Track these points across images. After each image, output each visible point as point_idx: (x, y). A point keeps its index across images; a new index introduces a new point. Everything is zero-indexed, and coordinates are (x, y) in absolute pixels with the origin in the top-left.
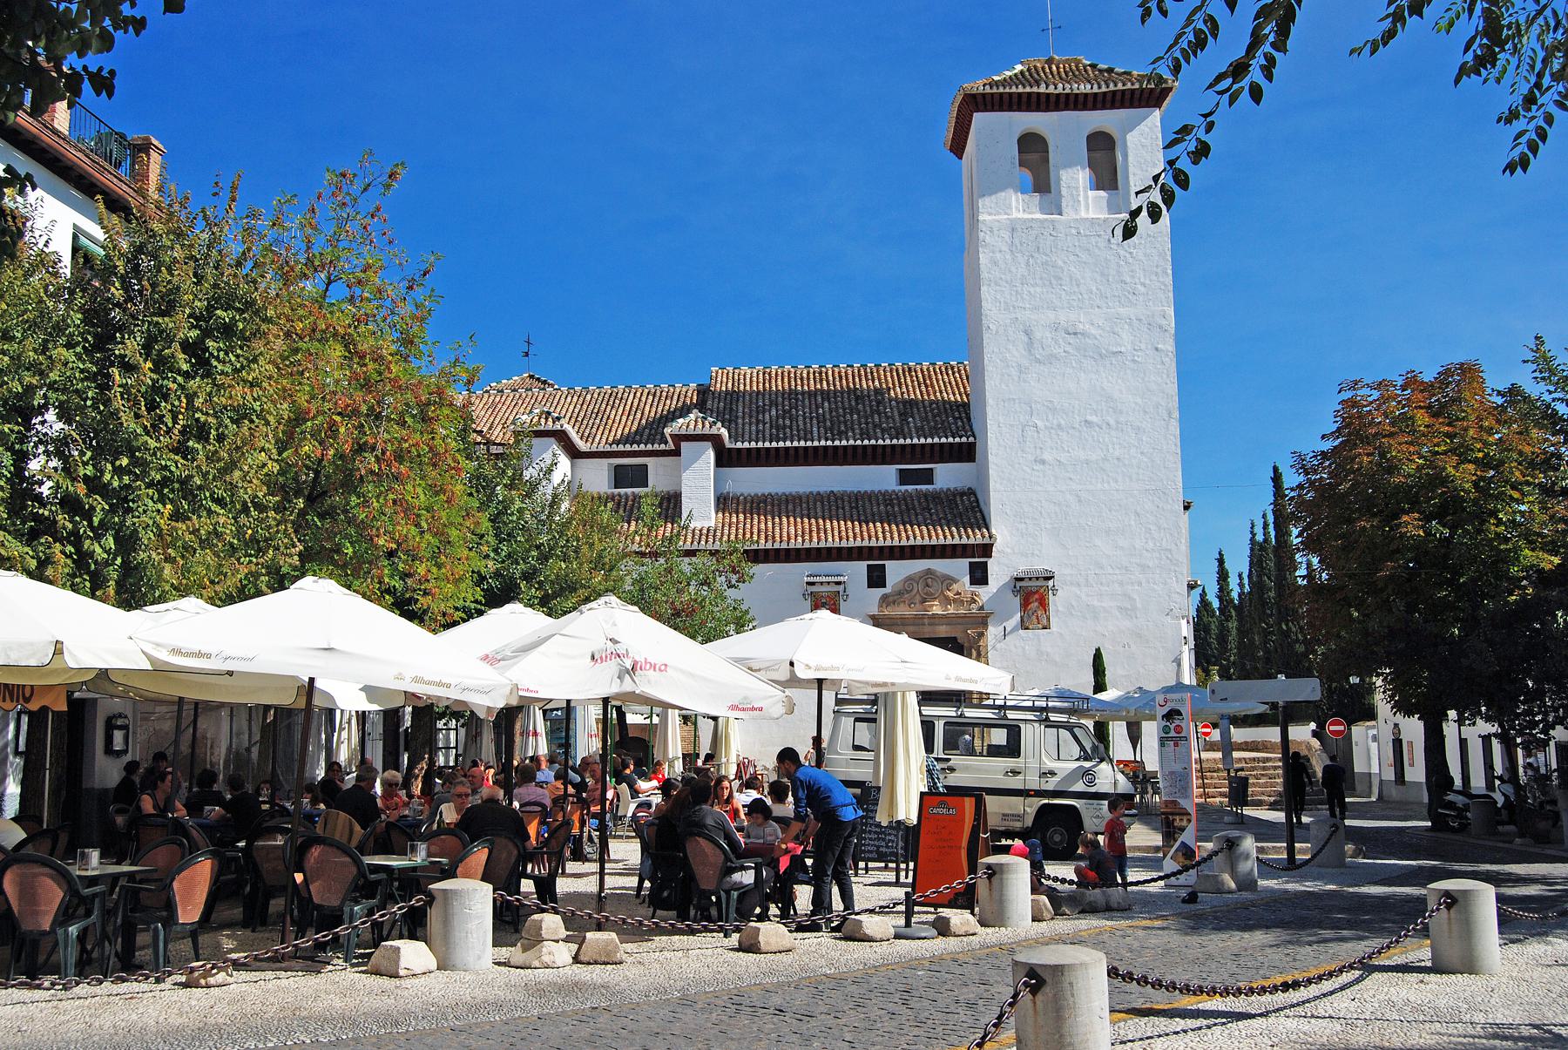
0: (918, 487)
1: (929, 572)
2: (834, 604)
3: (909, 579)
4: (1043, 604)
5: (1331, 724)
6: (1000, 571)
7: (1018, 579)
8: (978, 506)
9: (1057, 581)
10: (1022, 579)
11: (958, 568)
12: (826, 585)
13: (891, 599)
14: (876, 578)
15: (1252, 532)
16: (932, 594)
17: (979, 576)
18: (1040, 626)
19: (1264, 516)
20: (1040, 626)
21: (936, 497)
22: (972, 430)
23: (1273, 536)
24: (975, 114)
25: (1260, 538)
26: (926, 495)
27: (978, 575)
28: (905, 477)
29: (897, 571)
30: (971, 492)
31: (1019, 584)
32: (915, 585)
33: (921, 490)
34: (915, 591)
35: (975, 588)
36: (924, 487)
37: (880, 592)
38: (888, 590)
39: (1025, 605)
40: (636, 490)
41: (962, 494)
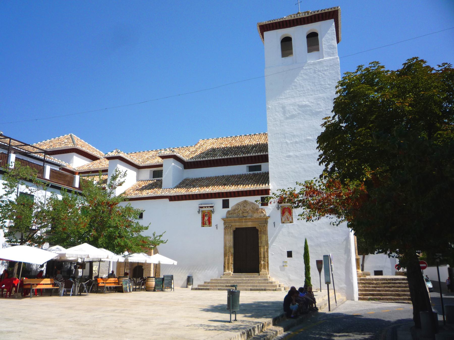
0: (254, 172)
1: (245, 202)
2: (210, 215)
3: (238, 205)
13: (231, 212)
14: (226, 205)
16: (246, 210)
18: (289, 222)
20: (289, 222)
28: (251, 169)
29: (233, 202)
32: (240, 207)
33: (255, 173)
35: (263, 207)
36: (256, 172)
37: (226, 210)
39: (283, 213)
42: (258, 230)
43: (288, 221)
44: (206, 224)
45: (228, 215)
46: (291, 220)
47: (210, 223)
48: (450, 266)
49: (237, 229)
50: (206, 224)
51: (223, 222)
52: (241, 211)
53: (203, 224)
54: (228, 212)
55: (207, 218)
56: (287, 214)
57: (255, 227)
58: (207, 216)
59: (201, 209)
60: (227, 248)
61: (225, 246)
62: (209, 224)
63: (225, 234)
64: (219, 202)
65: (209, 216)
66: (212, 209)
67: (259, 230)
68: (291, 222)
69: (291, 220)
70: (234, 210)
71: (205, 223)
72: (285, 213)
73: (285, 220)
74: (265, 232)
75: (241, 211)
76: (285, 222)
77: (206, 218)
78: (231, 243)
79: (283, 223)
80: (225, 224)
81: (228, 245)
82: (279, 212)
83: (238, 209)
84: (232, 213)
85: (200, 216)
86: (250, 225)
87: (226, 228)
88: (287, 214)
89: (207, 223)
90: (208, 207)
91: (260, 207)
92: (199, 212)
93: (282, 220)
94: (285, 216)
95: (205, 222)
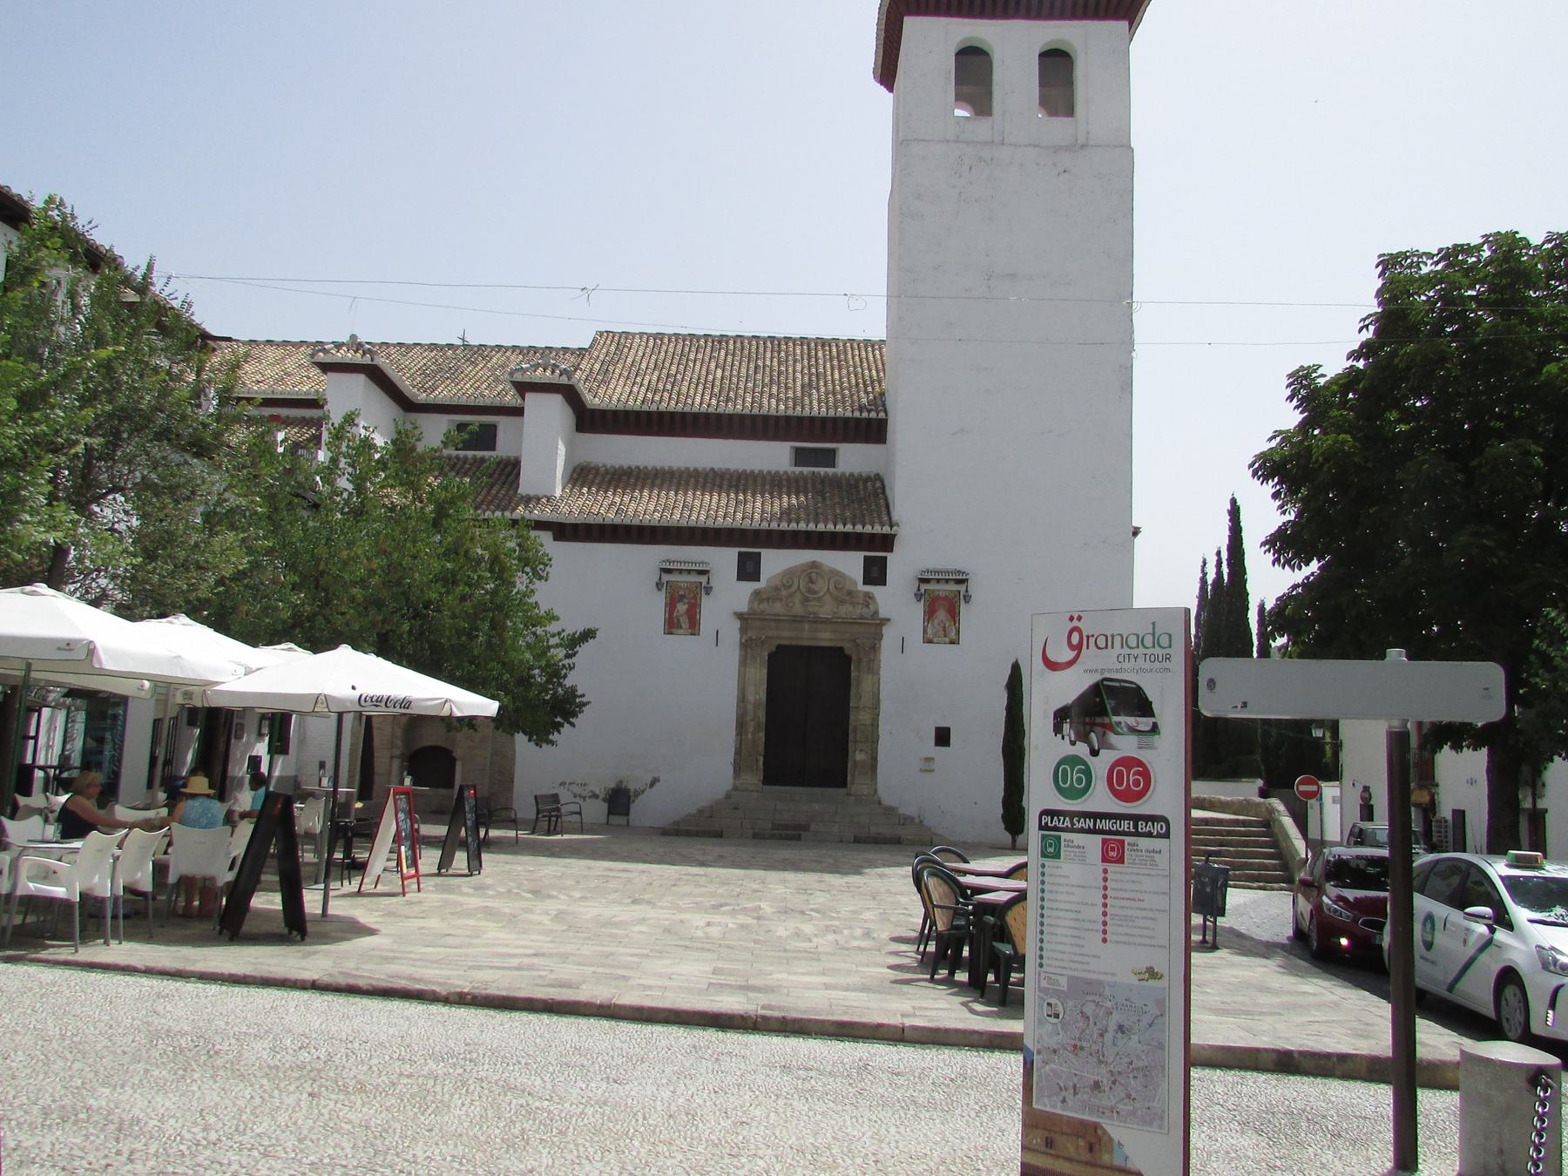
1: (814, 565)
2: (695, 598)
3: (790, 573)
4: (954, 614)
5: (1301, 783)
6: (901, 565)
7: (923, 581)
8: (884, 492)
9: (974, 589)
10: (927, 581)
11: (850, 564)
12: (694, 574)
13: (764, 597)
14: (748, 569)
15: (1203, 571)
16: (816, 592)
17: (876, 573)
18: (947, 640)
19: (1219, 553)
20: (947, 640)
21: (838, 483)
22: (884, 405)
23: (1226, 577)
24: (906, 18)
25: (1211, 577)
26: (824, 480)
27: (875, 572)
29: (775, 562)
30: (878, 478)
31: (924, 587)
34: (795, 587)
37: (751, 586)
38: (762, 584)
39: (930, 614)
40: (479, 454)
41: (868, 479)
42: (848, 659)
43: (945, 636)
44: (681, 627)
45: (756, 604)
46: (953, 635)
47: (694, 627)
48: (1264, 784)
49: (779, 647)
50: (681, 627)
51: (737, 624)
52: (798, 594)
53: (671, 626)
54: (757, 594)
55: (686, 607)
56: (941, 615)
57: (842, 649)
58: (685, 601)
59: (666, 578)
60: (750, 707)
61: (742, 699)
62: (690, 628)
63: (743, 663)
64: (724, 560)
65: (693, 601)
66: (703, 579)
67: (854, 657)
68: (952, 642)
69: (953, 635)
70: (777, 589)
71: (676, 621)
72: (938, 613)
73: (935, 635)
74: (873, 669)
75: (798, 594)
76: (935, 640)
77: (682, 608)
78: (758, 693)
79: (930, 642)
80: (743, 630)
81: (751, 698)
82: (919, 610)
83: (790, 587)
84: (768, 599)
85: (659, 600)
86: (825, 638)
87: (746, 646)
88: (941, 615)
89: (685, 622)
90: (689, 571)
91: (862, 587)
92: (659, 585)
93: (925, 631)
94: (936, 622)
95: (678, 621)
